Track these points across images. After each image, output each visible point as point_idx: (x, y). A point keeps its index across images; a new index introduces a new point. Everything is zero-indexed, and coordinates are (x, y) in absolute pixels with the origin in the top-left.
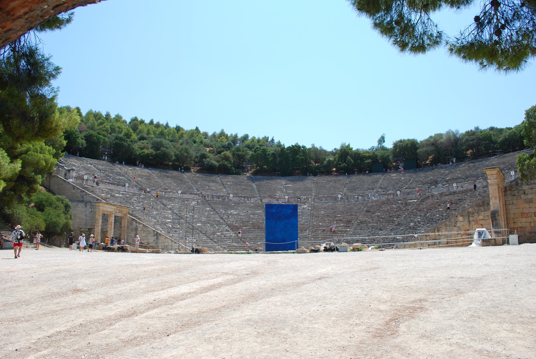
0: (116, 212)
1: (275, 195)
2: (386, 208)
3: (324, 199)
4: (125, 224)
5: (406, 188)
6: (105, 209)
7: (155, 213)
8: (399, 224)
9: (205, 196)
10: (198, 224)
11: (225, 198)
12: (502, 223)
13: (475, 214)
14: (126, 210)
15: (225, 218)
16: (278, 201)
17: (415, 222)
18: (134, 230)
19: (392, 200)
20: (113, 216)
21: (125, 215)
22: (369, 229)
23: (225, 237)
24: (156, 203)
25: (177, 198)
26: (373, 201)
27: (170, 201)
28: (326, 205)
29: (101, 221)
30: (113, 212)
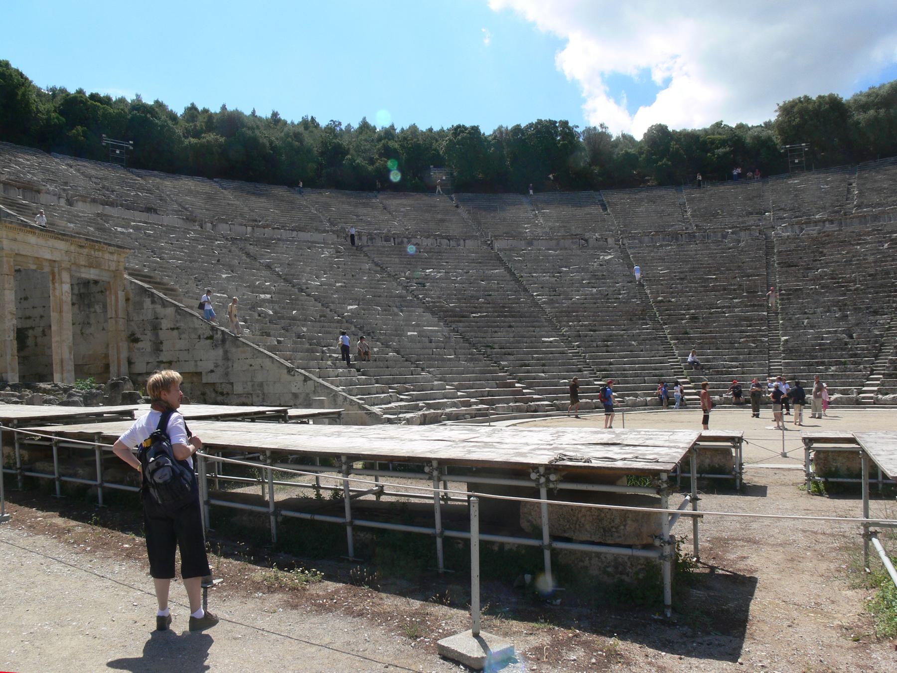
1: (520, 233)
3: (646, 239)
4: (117, 305)
7: (224, 276)
11: (402, 242)
14: (115, 257)
15: (416, 289)
18: (150, 328)
24: (230, 251)
25: (283, 240)
27: (268, 246)
28: (661, 252)
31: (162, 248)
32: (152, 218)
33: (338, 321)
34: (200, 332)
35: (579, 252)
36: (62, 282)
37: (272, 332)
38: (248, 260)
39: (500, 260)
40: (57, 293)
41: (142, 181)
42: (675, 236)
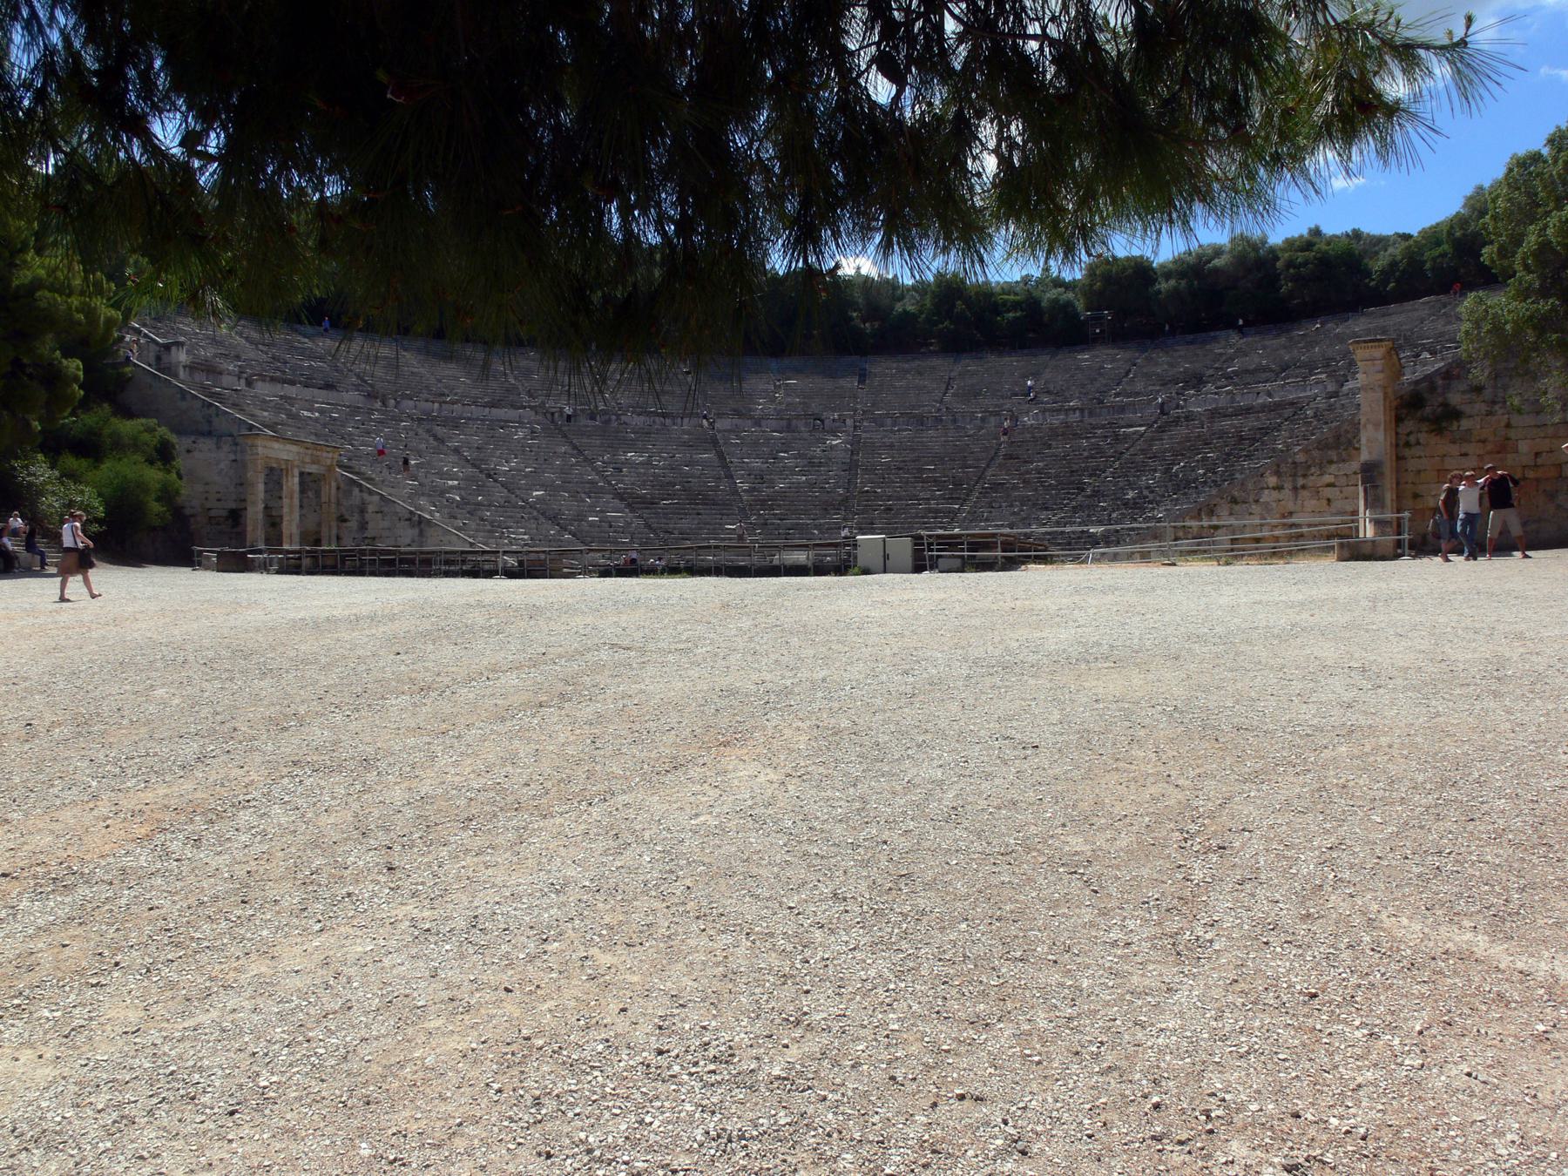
0: (303, 462)
1: (750, 410)
2: (1060, 447)
3: (889, 421)
5: (1117, 395)
6: (272, 454)
8: (1097, 494)
9: (553, 414)
10: (535, 494)
11: (610, 420)
12: (1389, 497)
13: (1313, 470)
14: (330, 455)
15: (611, 475)
16: (760, 426)
17: (1140, 488)
19: (1078, 426)
20: (296, 472)
21: (330, 469)
22: (1012, 506)
23: (611, 526)
26: (1025, 428)
27: (456, 427)
29: (261, 487)
30: (296, 463)
31: (350, 434)
32: (331, 396)
33: (522, 507)
34: (400, 515)
35: (806, 435)
36: (293, 476)
37: (459, 516)
38: (435, 443)
39: (715, 442)
40: (290, 484)
41: (310, 345)
42: (921, 421)
